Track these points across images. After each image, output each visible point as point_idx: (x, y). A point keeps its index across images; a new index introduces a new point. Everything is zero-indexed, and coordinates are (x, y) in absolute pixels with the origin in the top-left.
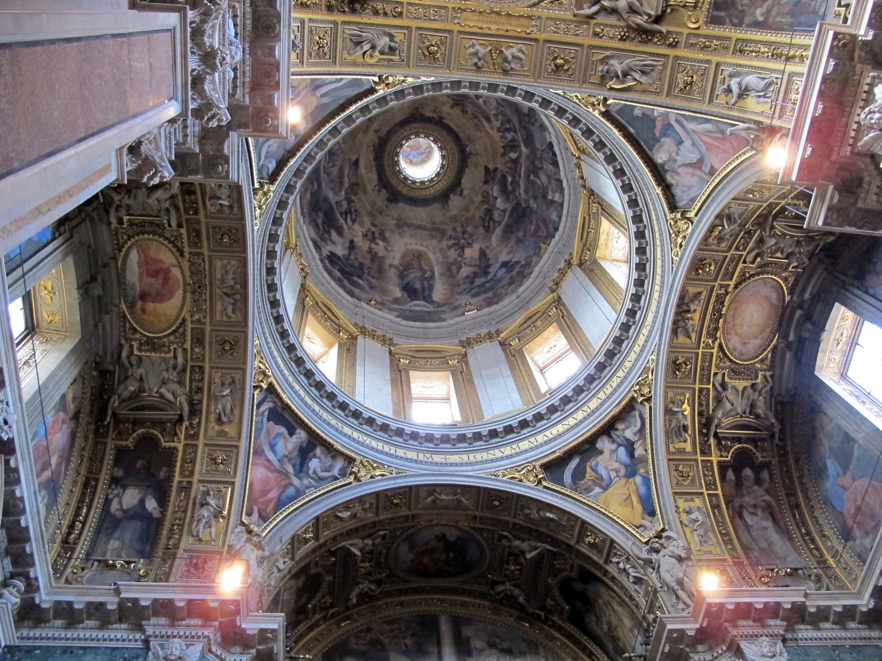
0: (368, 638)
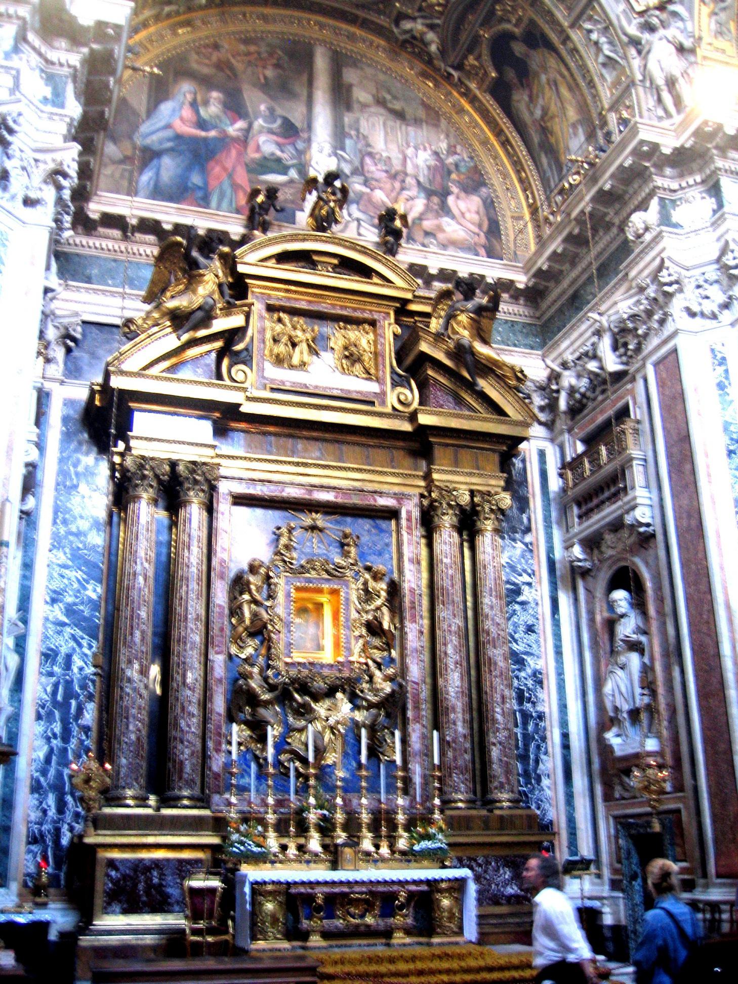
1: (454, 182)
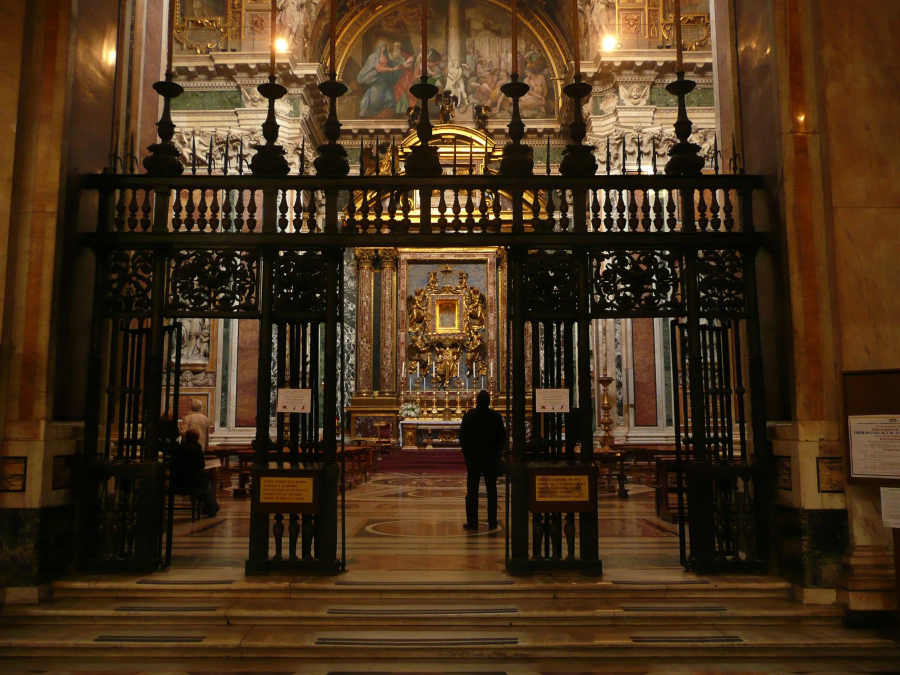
0: (395, 21)
1: (528, 69)
